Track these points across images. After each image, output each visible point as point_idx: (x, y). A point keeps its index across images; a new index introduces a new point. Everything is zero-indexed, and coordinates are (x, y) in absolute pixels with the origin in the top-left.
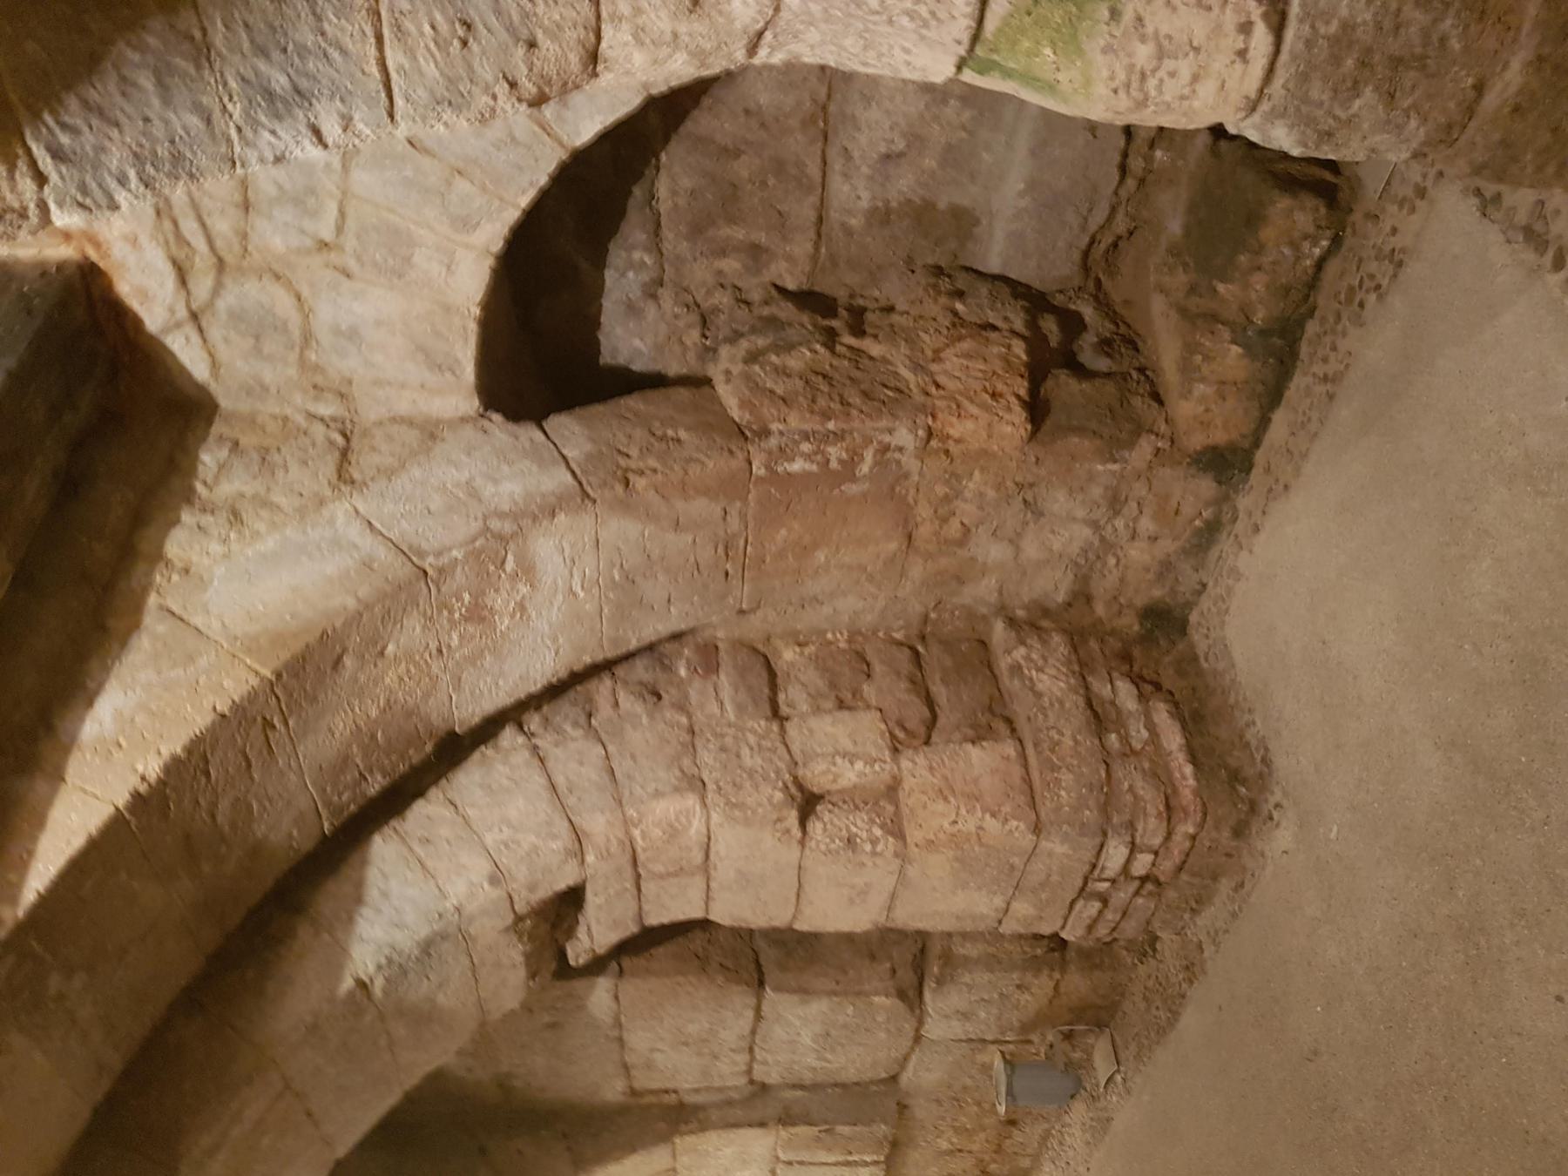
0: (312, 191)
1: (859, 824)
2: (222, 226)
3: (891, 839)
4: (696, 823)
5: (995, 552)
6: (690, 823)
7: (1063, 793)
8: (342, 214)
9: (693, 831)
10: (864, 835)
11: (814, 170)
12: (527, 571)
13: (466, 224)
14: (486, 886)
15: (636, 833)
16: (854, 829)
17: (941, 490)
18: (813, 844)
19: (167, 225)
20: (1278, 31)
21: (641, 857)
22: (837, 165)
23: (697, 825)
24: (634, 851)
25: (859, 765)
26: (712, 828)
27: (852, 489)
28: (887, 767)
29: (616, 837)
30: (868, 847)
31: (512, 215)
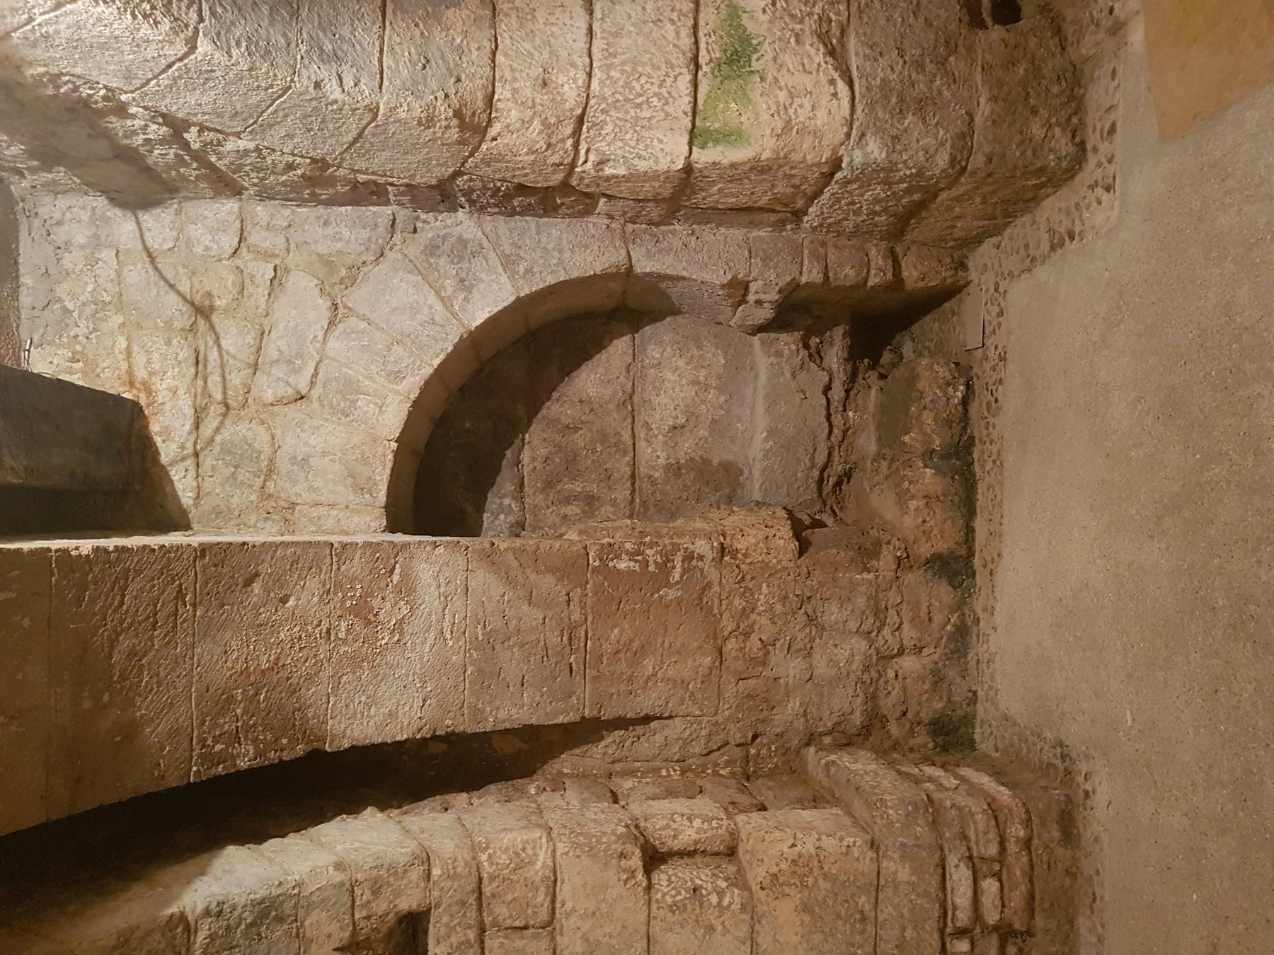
0: (299, 355)
1: (702, 875)
2: (235, 380)
3: (736, 891)
4: (541, 856)
5: (792, 669)
6: (536, 855)
7: (891, 812)
8: (316, 374)
9: (539, 864)
10: (709, 886)
11: (626, 437)
12: (407, 589)
13: (397, 376)
14: (331, 870)
15: (484, 857)
16: (698, 882)
17: (738, 603)
18: (659, 896)
19: (200, 383)
20: (851, 84)
21: (487, 890)
22: (641, 433)
23: (543, 858)
24: (480, 880)
25: (697, 823)
26: (559, 860)
27: (671, 594)
28: (725, 823)
29: (463, 858)
30: (714, 899)
31: (428, 371)
